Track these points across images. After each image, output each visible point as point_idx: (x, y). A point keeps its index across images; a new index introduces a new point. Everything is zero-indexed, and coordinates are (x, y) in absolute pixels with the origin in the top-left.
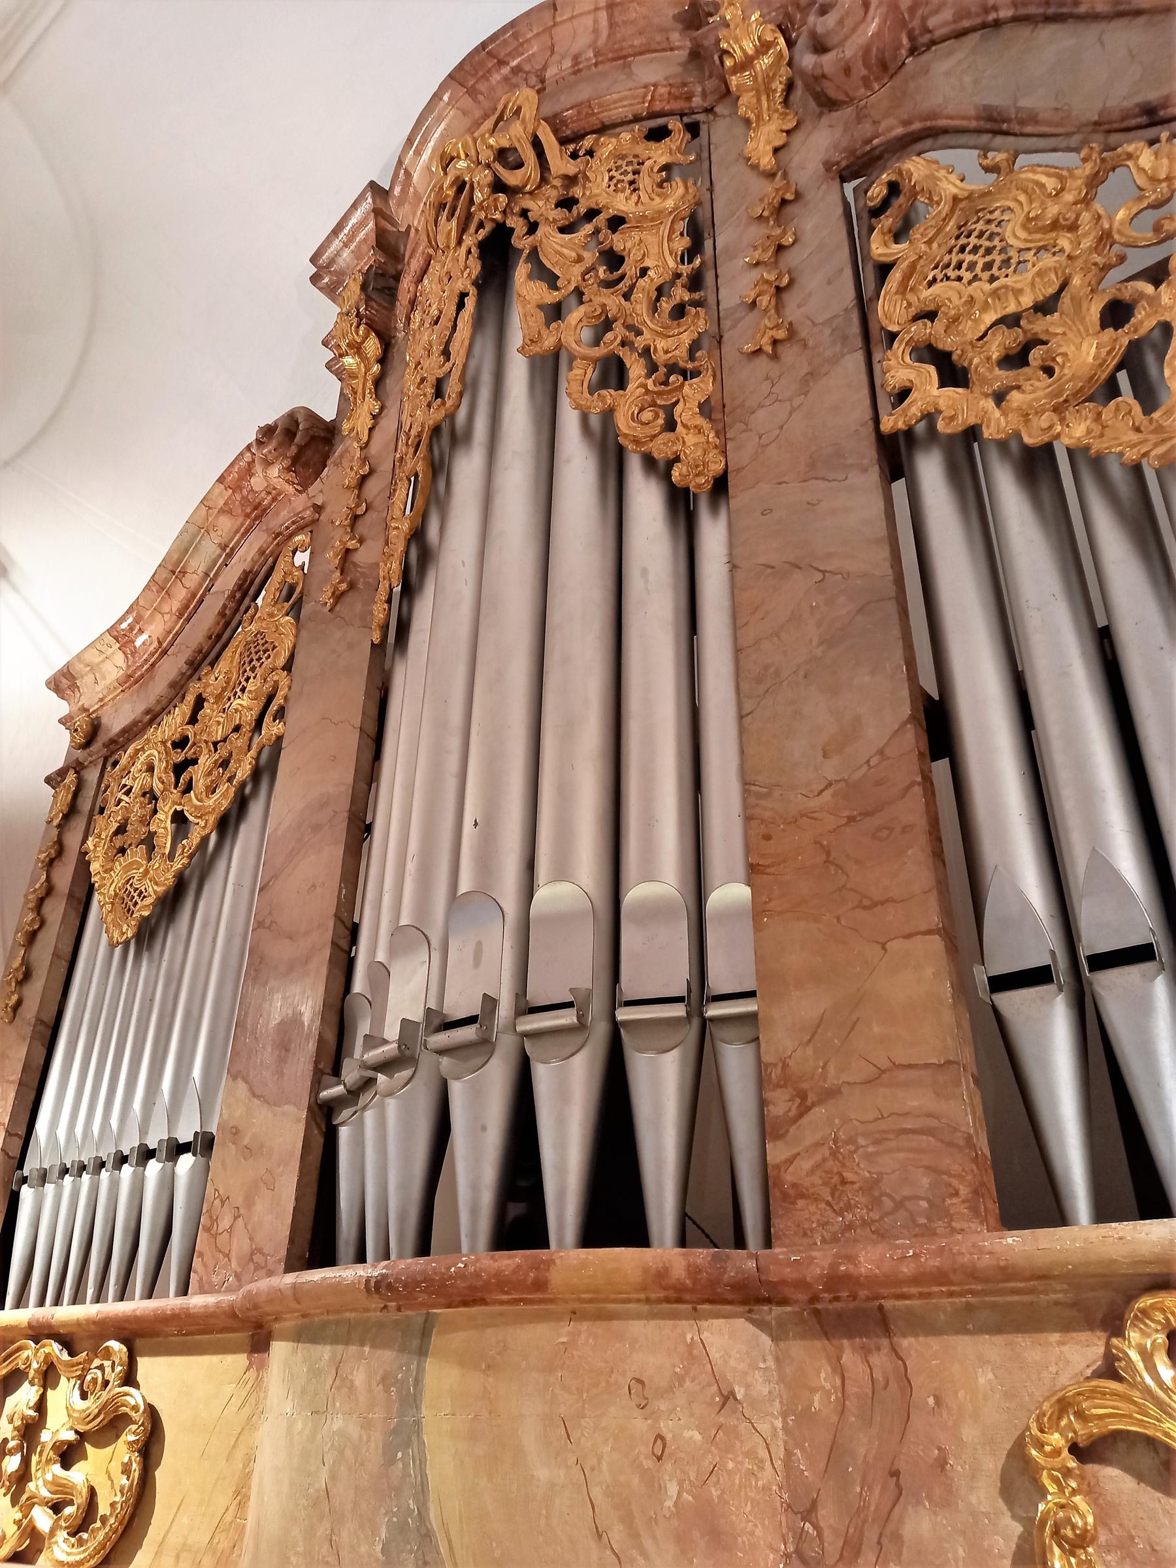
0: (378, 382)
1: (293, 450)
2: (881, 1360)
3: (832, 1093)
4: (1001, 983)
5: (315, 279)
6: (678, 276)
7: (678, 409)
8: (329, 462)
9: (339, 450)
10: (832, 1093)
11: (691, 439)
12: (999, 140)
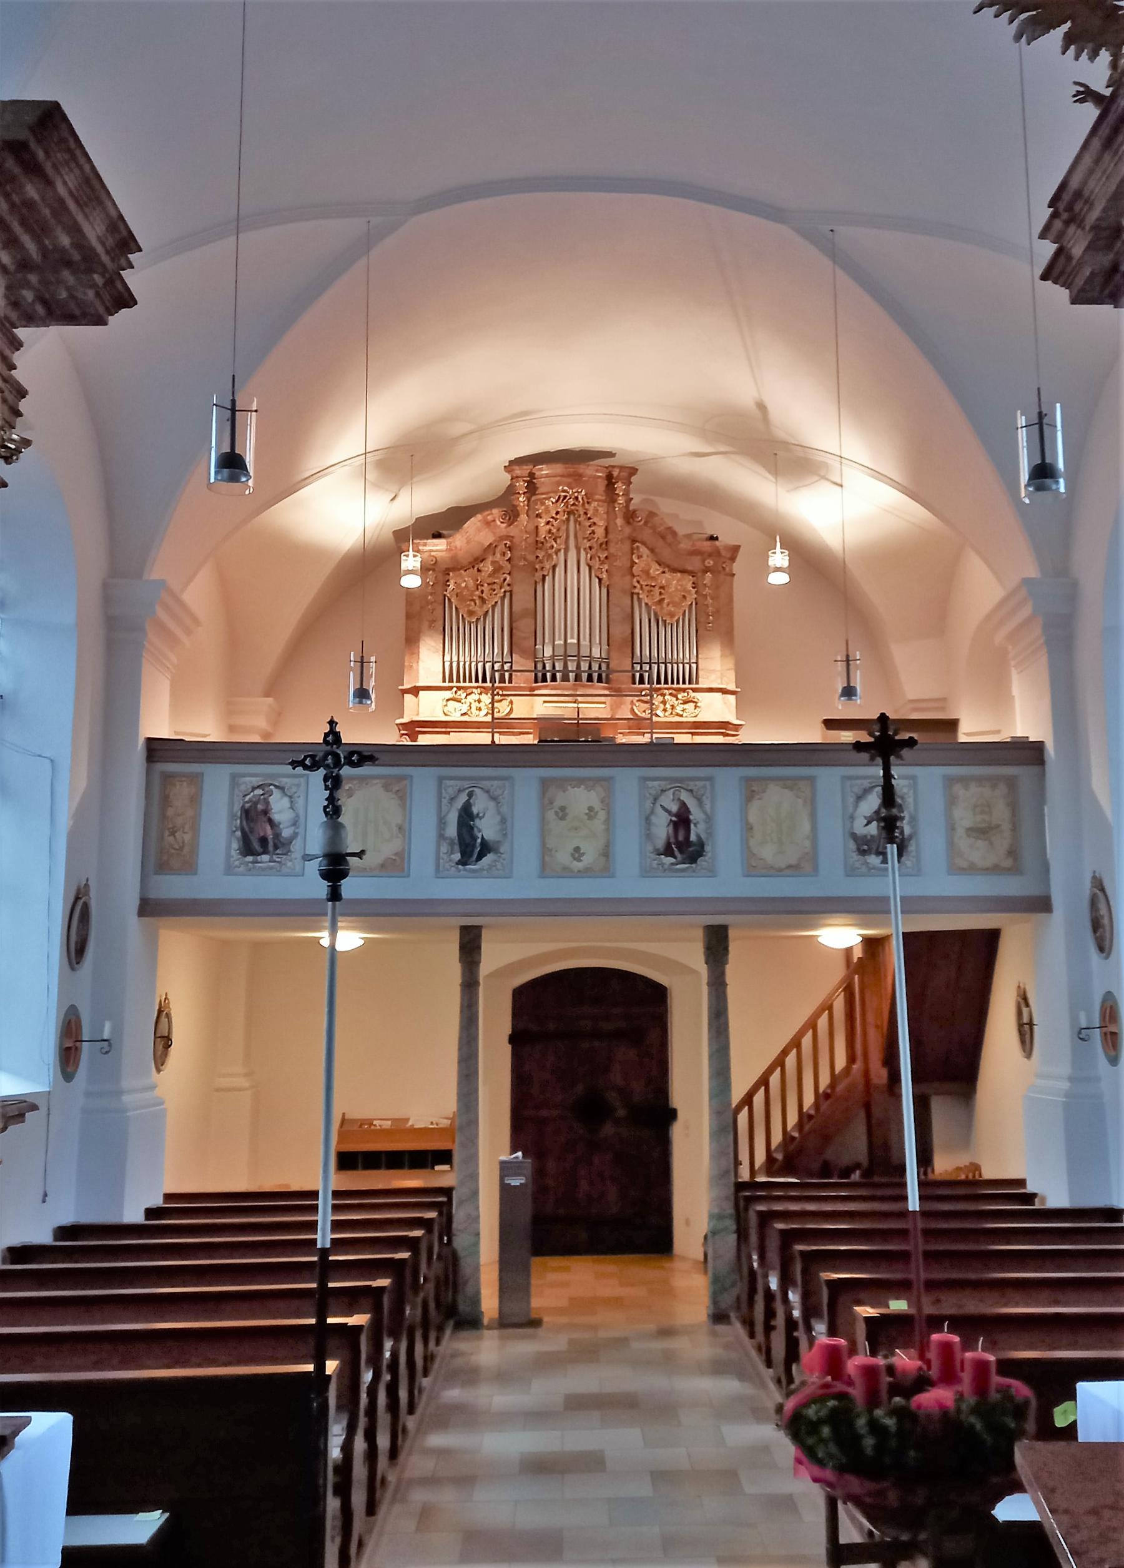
0: (527, 511)
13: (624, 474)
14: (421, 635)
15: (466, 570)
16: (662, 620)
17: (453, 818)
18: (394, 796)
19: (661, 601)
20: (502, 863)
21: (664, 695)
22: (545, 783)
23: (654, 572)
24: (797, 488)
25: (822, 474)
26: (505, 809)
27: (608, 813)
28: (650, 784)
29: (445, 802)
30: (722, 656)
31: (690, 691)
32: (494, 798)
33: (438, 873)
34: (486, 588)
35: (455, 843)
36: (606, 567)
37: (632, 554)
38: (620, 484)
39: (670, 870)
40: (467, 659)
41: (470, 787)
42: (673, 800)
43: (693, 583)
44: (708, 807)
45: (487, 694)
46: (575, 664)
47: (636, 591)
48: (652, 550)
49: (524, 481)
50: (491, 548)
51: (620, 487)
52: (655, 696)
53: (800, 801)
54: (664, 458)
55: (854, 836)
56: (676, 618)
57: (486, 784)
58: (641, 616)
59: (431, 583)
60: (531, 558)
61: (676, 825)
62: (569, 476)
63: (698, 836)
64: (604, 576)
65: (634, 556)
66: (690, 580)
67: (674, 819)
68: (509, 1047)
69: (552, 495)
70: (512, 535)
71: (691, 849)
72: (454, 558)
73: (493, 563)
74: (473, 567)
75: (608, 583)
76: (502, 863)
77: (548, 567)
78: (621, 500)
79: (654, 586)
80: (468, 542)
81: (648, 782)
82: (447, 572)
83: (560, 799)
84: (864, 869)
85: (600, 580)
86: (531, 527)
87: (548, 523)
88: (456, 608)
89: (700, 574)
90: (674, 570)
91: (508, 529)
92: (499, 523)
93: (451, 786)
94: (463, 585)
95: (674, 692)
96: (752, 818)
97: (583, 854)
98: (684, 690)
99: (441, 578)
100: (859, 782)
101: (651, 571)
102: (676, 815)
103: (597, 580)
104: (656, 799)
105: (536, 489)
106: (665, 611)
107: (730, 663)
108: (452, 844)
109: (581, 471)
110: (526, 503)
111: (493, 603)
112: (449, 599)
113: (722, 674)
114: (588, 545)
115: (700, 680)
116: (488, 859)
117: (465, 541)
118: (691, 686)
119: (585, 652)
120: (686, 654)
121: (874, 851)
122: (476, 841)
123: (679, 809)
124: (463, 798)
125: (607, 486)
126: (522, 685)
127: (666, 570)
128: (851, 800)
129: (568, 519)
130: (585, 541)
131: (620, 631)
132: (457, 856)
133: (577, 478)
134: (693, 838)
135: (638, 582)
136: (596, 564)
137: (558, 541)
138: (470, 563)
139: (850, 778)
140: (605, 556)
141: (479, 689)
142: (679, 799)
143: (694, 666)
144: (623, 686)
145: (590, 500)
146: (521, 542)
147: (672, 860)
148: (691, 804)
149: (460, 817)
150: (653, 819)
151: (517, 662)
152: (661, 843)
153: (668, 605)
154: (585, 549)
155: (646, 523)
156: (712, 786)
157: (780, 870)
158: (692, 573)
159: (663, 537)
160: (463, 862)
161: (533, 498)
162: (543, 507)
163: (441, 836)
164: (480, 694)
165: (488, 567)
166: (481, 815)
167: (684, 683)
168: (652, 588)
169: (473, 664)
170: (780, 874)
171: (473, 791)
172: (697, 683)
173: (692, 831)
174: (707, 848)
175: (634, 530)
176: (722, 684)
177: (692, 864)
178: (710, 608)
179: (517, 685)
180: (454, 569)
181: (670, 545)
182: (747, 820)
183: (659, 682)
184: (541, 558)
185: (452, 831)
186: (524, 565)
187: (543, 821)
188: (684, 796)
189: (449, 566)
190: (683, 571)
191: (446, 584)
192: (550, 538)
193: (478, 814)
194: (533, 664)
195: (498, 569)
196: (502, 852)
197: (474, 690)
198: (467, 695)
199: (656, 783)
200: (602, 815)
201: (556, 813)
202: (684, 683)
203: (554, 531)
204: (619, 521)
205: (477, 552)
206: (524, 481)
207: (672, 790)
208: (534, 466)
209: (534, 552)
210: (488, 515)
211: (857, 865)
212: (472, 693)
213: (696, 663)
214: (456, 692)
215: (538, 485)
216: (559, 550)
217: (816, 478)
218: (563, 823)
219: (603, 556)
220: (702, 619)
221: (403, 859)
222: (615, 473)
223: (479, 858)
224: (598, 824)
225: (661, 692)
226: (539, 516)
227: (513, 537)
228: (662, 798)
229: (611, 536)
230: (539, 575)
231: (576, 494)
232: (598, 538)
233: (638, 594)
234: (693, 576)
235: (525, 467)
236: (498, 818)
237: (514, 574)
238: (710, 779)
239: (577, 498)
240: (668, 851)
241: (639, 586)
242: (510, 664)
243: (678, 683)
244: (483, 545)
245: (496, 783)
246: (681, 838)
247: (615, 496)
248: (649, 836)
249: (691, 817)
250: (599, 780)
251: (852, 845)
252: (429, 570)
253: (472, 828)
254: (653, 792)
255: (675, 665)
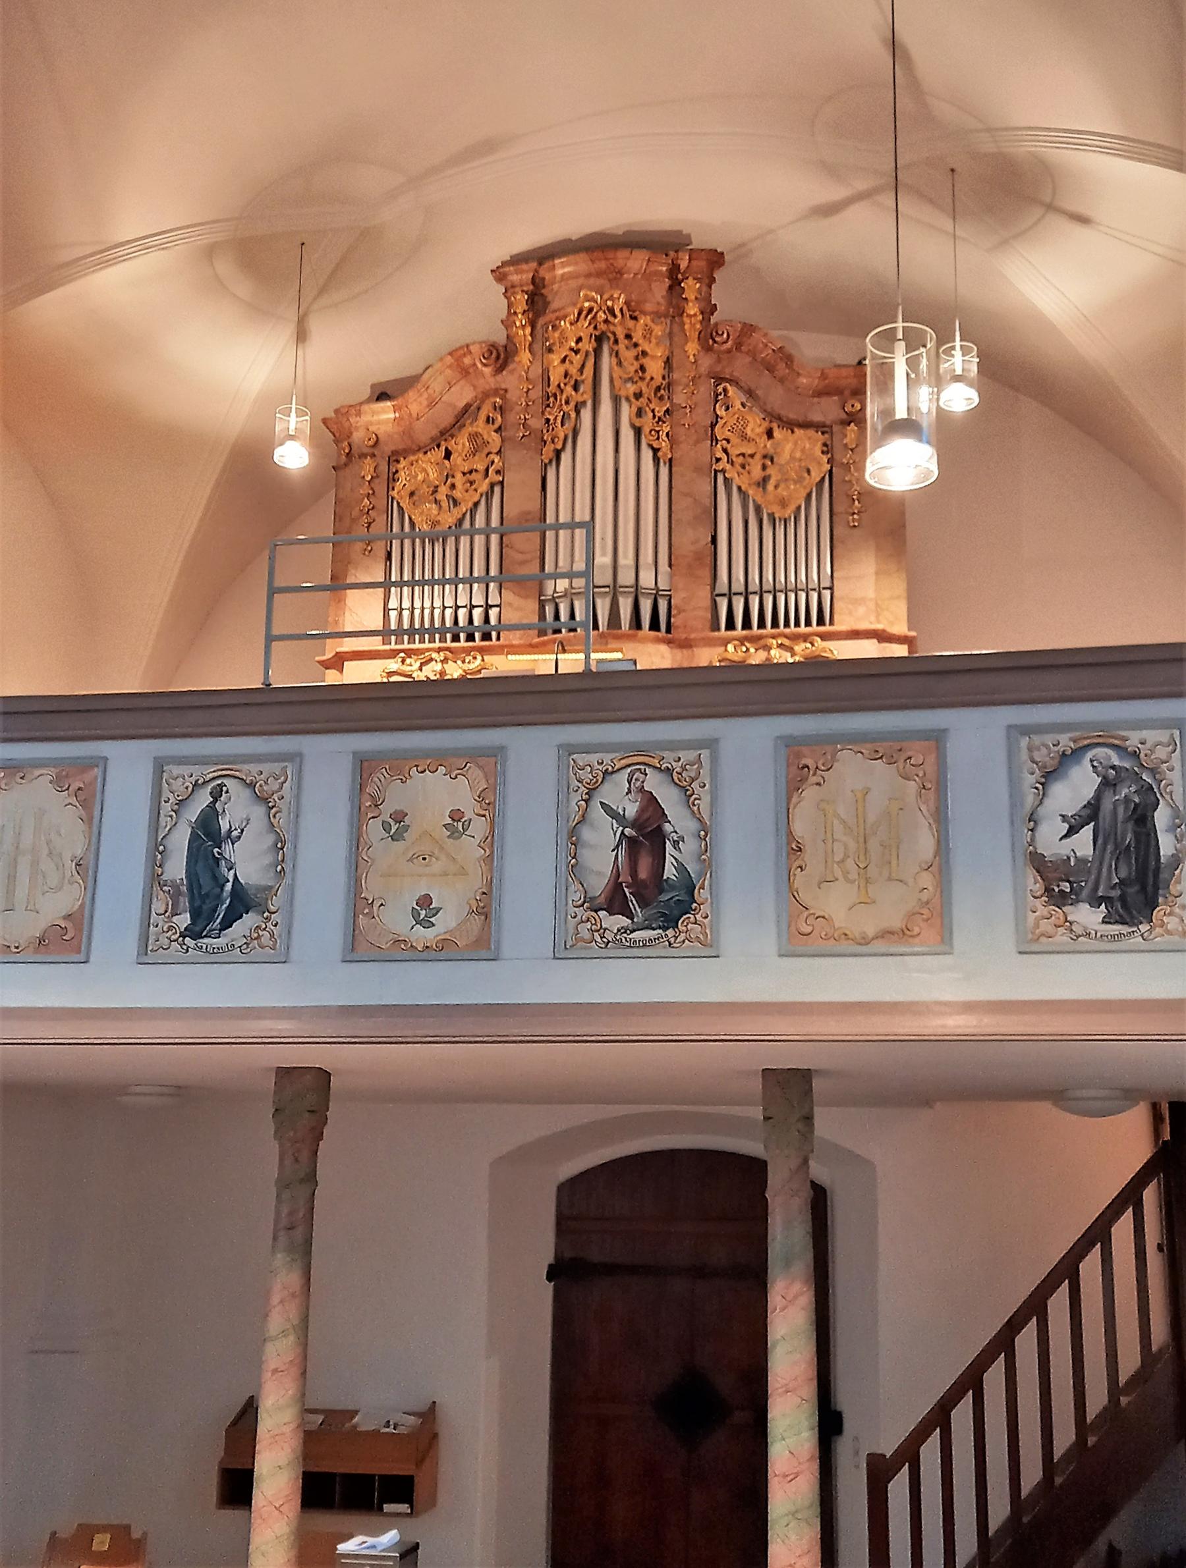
1: (498, 365)
2: (690, 651)
3: (684, 611)
4: (718, 595)
5: (492, 271)
6: (662, 384)
7: (661, 433)
8: (507, 369)
9: (511, 366)
10: (684, 611)
11: (664, 444)
12: (751, 399)
13: (700, 264)
14: (350, 567)
15: (425, 453)
16: (769, 514)
17: (180, 841)
18: (73, 800)
19: (766, 480)
20: (272, 935)
21: (768, 648)
22: (364, 766)
23: (752, 430)
24: (1004, 243)
25: (1048, 200)
26: (282, 820)
27: (492, 822)
28: (582, 759)
29: (166, 808)
30: (877, 573)
31: (819, 639)
32: (263, 800)
33: (145, 953)
34: (459, 480)
35: (180, 893)
36: (666, 428)
37: (717, 401)
38: (690, 281)
39: (620, 944)
40: (427, 604)
41: (214, 779)
42: (629, 791)
43: (825, 445)
44: (704, 806)
45: (456, 662)
46: (608, 601)
47: (720, 466)
48: (750, 393)
49: (523, 291)
50: (465, 414)
51: (691, 287)
52: (752, 650)
53: (912, 786)
54: (771, 231)
55: (1038, 862)
56: (793, 507)
57: (250, 770)
58: (729, 512)
59: (369, 478)
60: (536, 423)
61: (632, 844)
62: (599, 274)
63: (681, 868)
64: (664, 444)
65: (717, 406)
66: (817, 441)
67: (628, 831)
68: (547, 1290)
69: (569, 310)
70: (504, 386)
71: (664, 897)
72: (408, 432)
73: (474, 437)
74: (438, 446)
75: (669, 456)
76: (272, 935)
77: (562, 436)
78: (692, 309)
79: (752, 456)
80: (432, 404)
81: (574, 756)
82: (394, 457)
83: (396, 797)
84: (1062, 937)
85: (655, 451)
86: (536, 371)
87: (563, 361)
88: (410, 518)
89: (836, 428)
90: (791, 425)
91: (499, 377)
92: (479, 365)
93: (180, 778)
94: (420, 477)
95: (786, 642)
96: (800, 828)
97: (438, 910)
98: (805, 638)
99: (384, 467)
100: (1049, 739)
101: (748, 431)
102: (636, 824)
103: (650, 453)
104: (591, 792)
105: (546, 304)
106: (771, 497)
107: (897, 586)
108: (175, 895)
109: (619, 263)
110: (528, 330)
111: (470, 505)
112: (398, 503)
113: (877, 605)
114: (631, 388)
115: (836, 617)
116: (249, 920)
117: (425, 403)
118: (821, 629)
119: (626, 578)
120: (813, 572)
121: (1085, 894)
122: (222, 887)
123: (642, 811)
124: (203, 799)
125: (671, 288)
126: (514, 642)
127: (775, 425)
128: (1029, 780)
129: (598, 352)
130: (629, 385)
131: (692, 538)
132: (184, 920)
133: (615, 276)
134: (670, 872)
135: (725, 451)
136: (647, 422)
137: (582, 389)
138: (433, 439)
139: (1027, 730)
140: (665, 408)
141: (441, 653)
142: (641, 790)
143: (827, 594)
144: (693, 636)
145: (636, 314)
146: (520, 398)
147: (625, 921)
148: (668, 798)
149: (194, 837)
150: (586, 834)
151: (510, 604)
152: (599, 885)
153: (776, 487)
154: (627, 399)
155: (738, 346)
156: (714, 759)
157: (865, 941)
158: (822, 427)
159: (771, 369)
160: (193, 932)
161: (541, 322)
162: (557, 335)
163: (155, 879)
164: (443, 662)
165: (460, 445)
166: (235, 834)
167: (808, 623)
168: (750, 460)
169: (437, 612)
170: (864, 949)
171: (221, 786)
172: (831, 623)
173: (669, 859)
174: (702, 895)
175: (719, 360)
176: (879, 622)
177: (665, 929)
178: (856, 487)
179: (507, 643)
180: (404, 453)
181: (782, 380)
182: (790, 833)
183: (762, 624)
184: (552, 421)
185: (176, 868)
186: (524, 436)
187: (357, 842)
188: (654, 783)
189: (401, 447)
190: (806, 425)
191: (392, 478)
192: (565, 384)
193: (230, 831)
194: (535, 606)
195: (478, 445)
196: (272, 908)
197: (434, 655)
198: (422, 664)
199: (594, 758)
200: (479, 827)
201: (386, 827)
202: (808, 623)
203: (573, 371)
204: (692, 348)
205: (447, 420)
206: (523, 291)
207: (629, 770)
208: (540, 264)
209: (543, 413)
210: (464, 355)
211: (1045, 925)
212: (431, 660)
213: (831, 588)
214: (403, 662)
215: (550, 298)
216: (584, 403)
217: (1038, 212)
218: (399, 845)
219: (660, 411)
220: (838, 508)
221: (79, 928)
222: (683, 265)
223: (227, 924)
224: (470, 848)
225: (762, 642)
226: (550, 350)
227: (506, 391)
228: (606, 787)
229: (676, 375)
230: (548, 450)
231: (609, 303)
232: (652, 379)
233: (723, 471)
234: (823, 433)
235: (524, 267)
236: (270, 839)
237: (508, 453)
238: (711, 744)
239: (611, 311)
240: (615, 902)
241: (725, 458)
242: (498, 609)
243: (797, 624)
244: (455, 407)
245: (267, 768)
246: (643, 874)
247: (683, 303)
248: (575, 869)
249: (668, 828)
250: (474, 755)
251: (1034, 884)
252: (363, 456)
253: (217, 861)
254: (586, 776)
255: (792, 596)
